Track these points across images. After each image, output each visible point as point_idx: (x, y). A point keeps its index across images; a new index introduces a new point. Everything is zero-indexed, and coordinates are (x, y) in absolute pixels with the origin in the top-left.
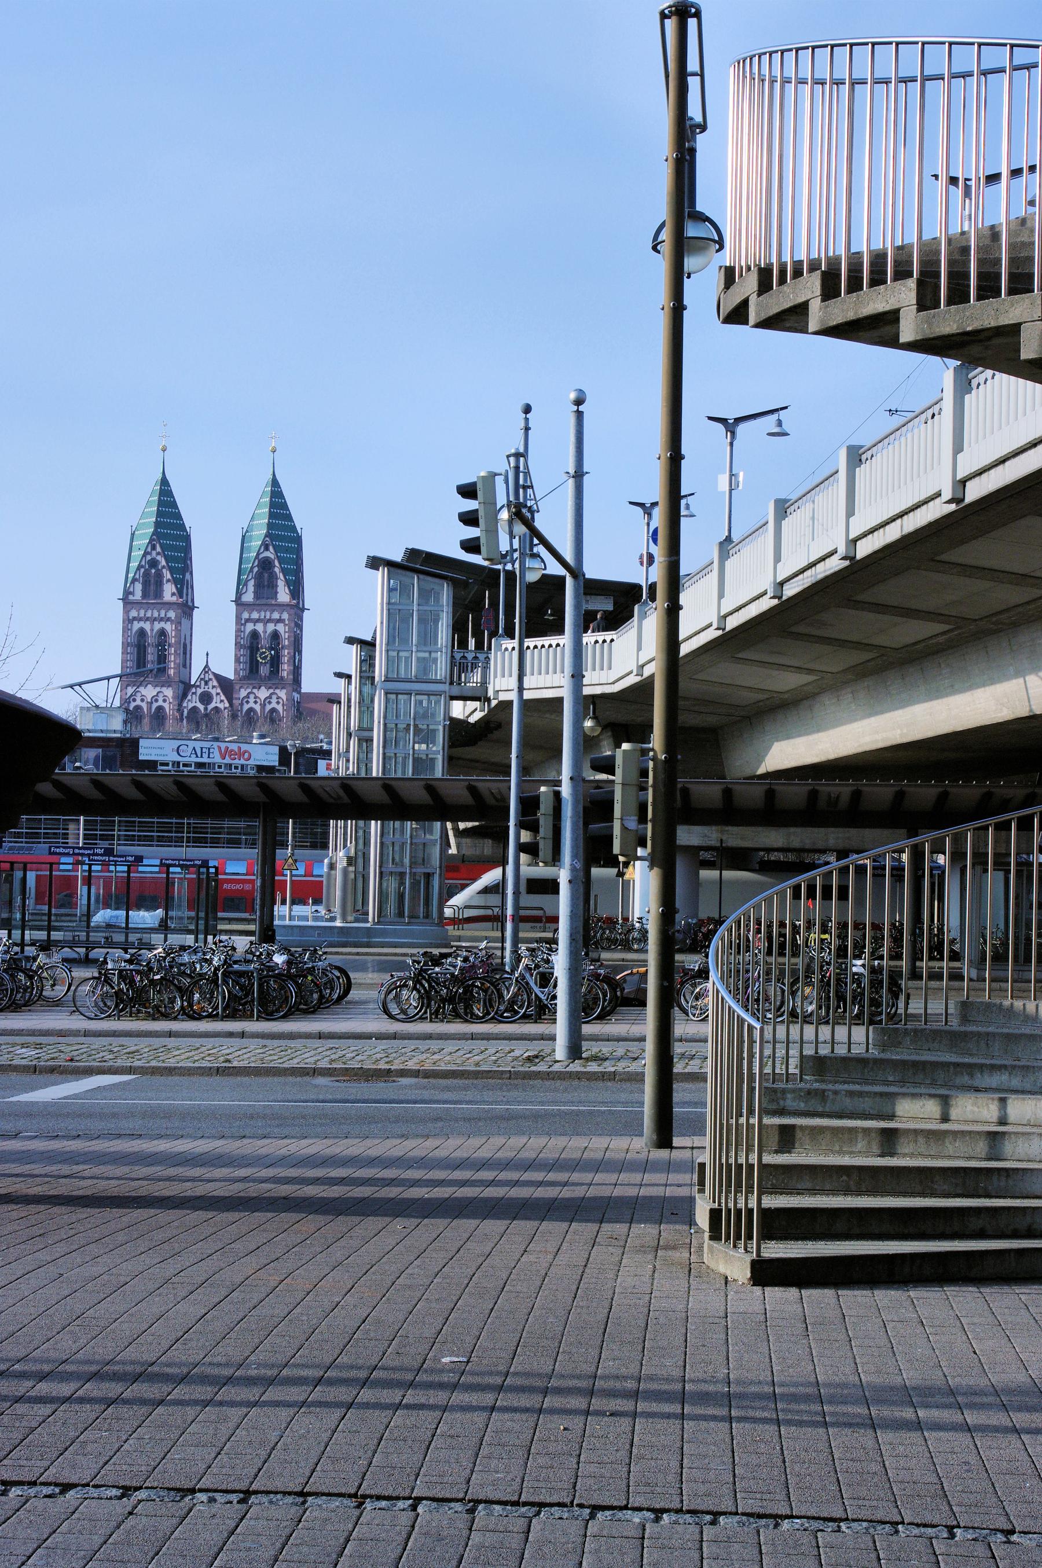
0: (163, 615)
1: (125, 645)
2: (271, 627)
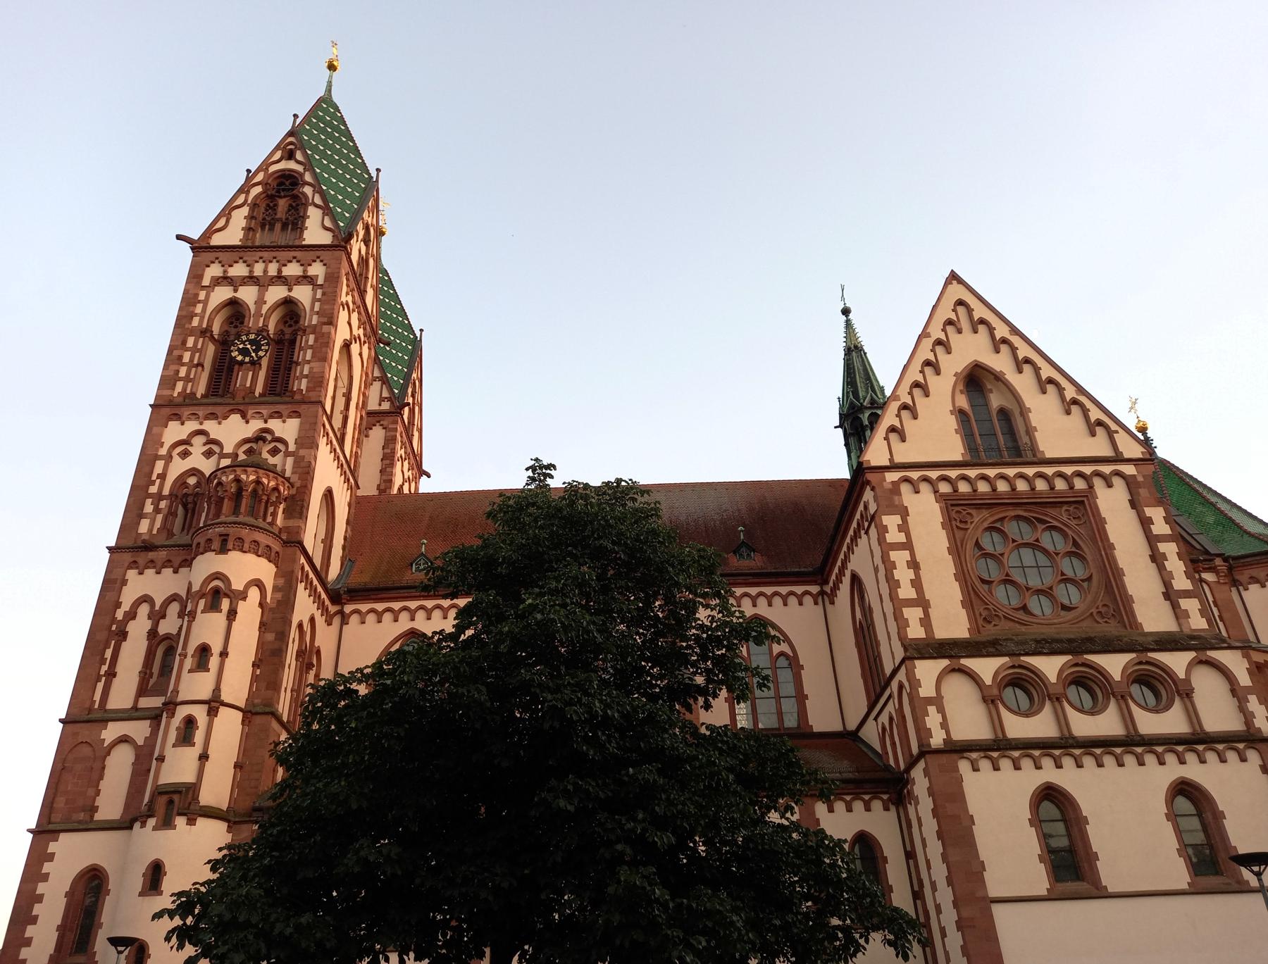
2: (276, 293)
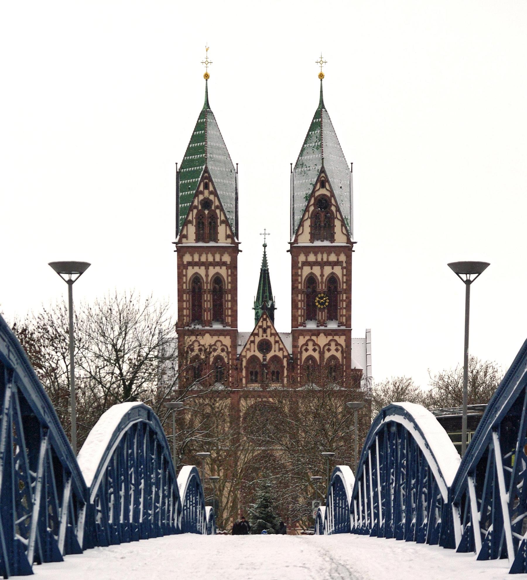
0: (217, 259)
1: (181, 292)
2: (328, 270)
